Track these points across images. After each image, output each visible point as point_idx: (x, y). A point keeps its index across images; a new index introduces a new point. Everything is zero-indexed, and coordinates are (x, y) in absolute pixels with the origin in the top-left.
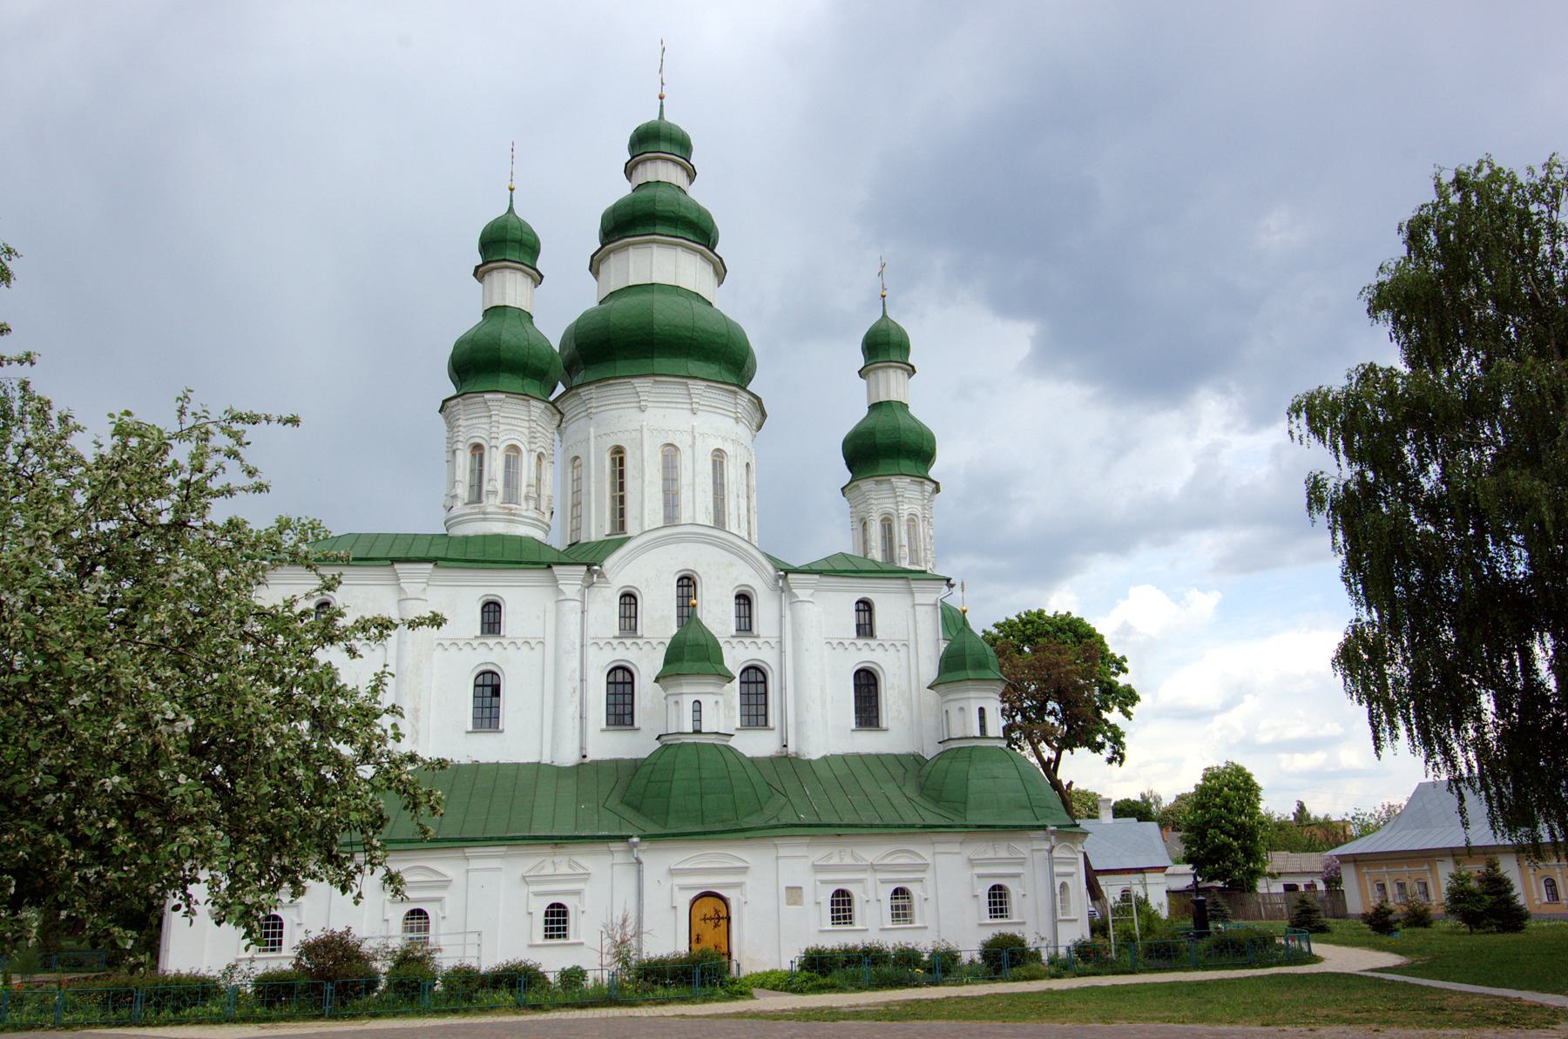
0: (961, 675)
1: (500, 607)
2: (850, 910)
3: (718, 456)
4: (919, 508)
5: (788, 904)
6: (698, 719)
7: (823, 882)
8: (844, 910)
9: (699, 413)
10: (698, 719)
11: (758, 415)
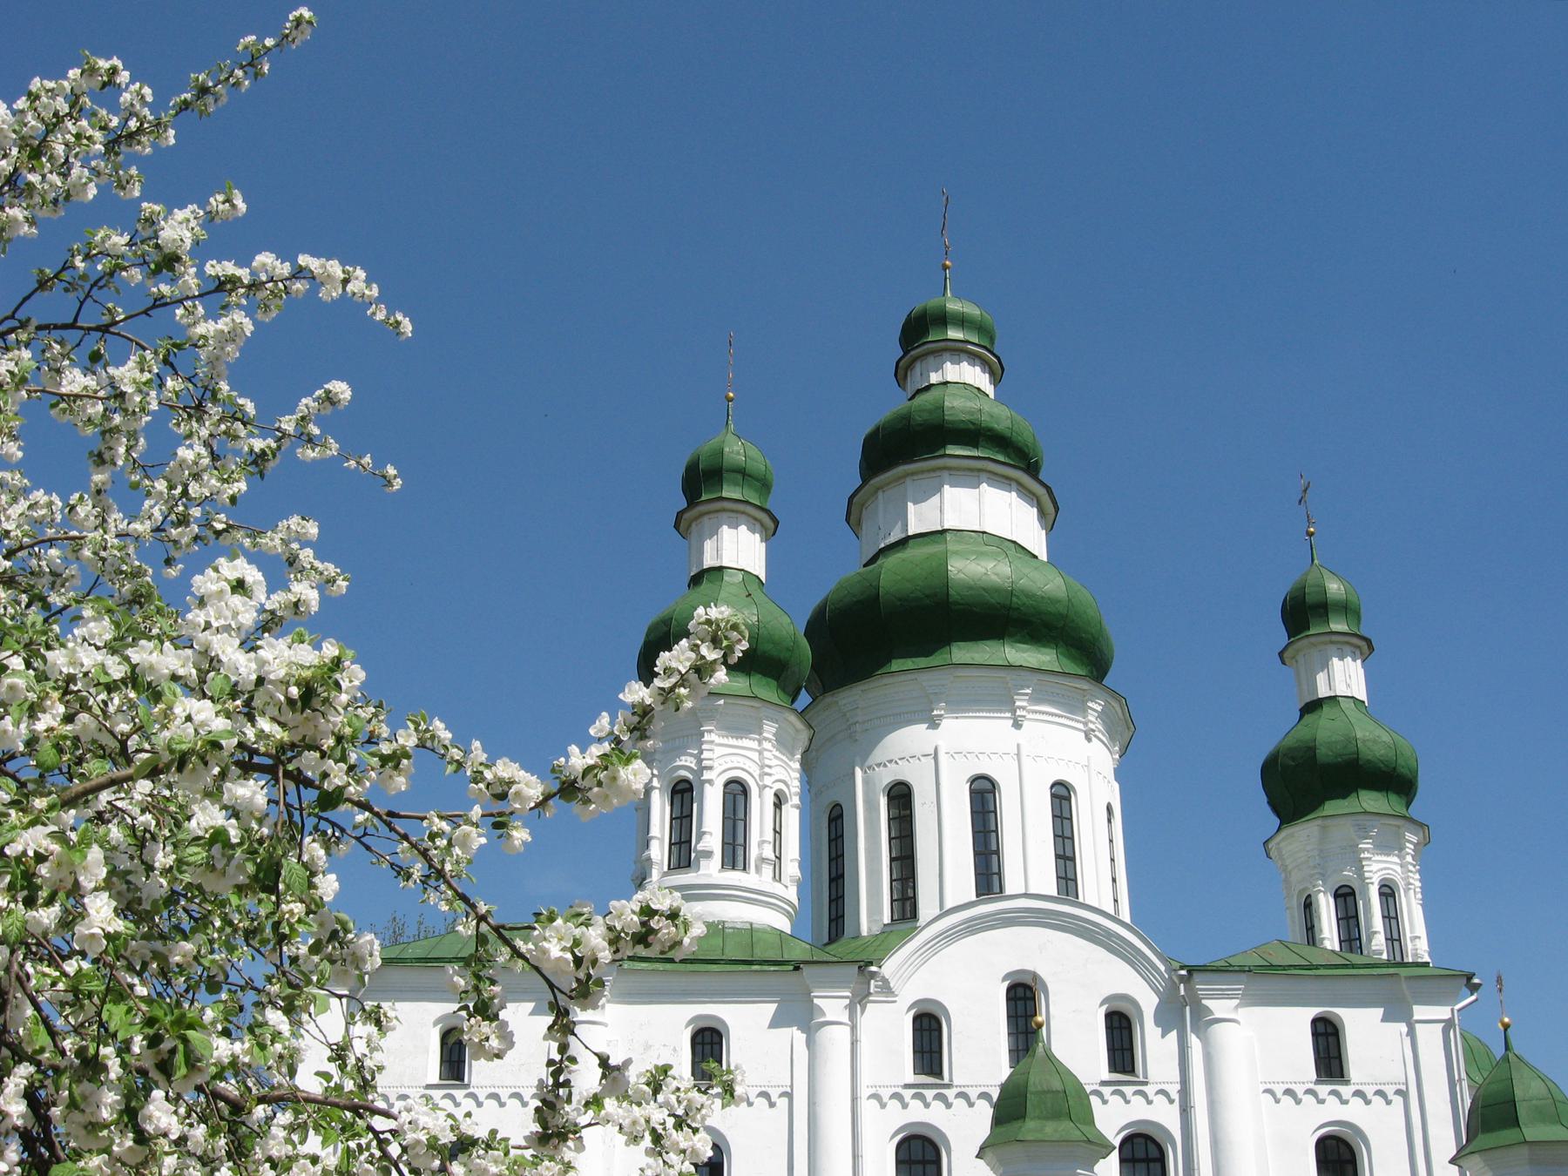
0: (1508, 1135)
1: (721, 1036)
3: (1062, 795)
4: (1398, 869)
9: (1026, 724)
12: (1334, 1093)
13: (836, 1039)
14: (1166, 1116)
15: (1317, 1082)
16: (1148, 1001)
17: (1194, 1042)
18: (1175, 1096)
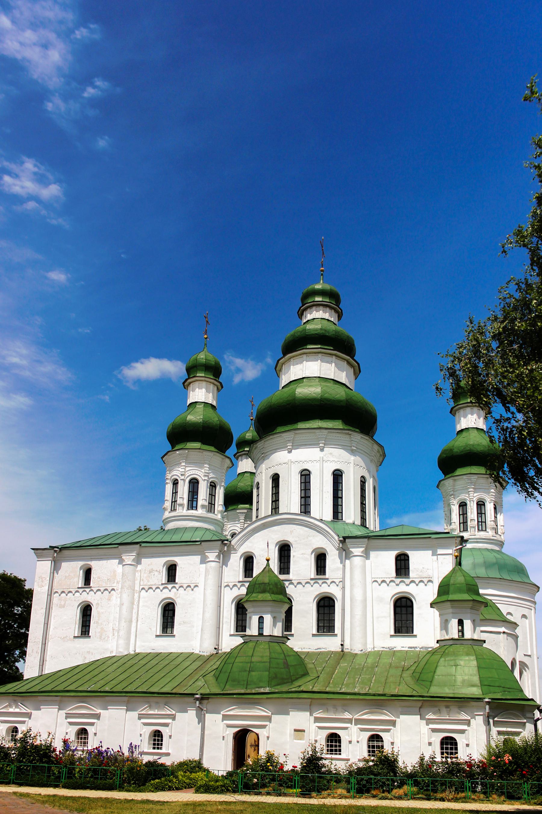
2: (340, 746)
6: (261, 628)
7: (320, 728)
8: (336, 746)
10: (261, 628)
11: (376, 447)
15: (396, 578)
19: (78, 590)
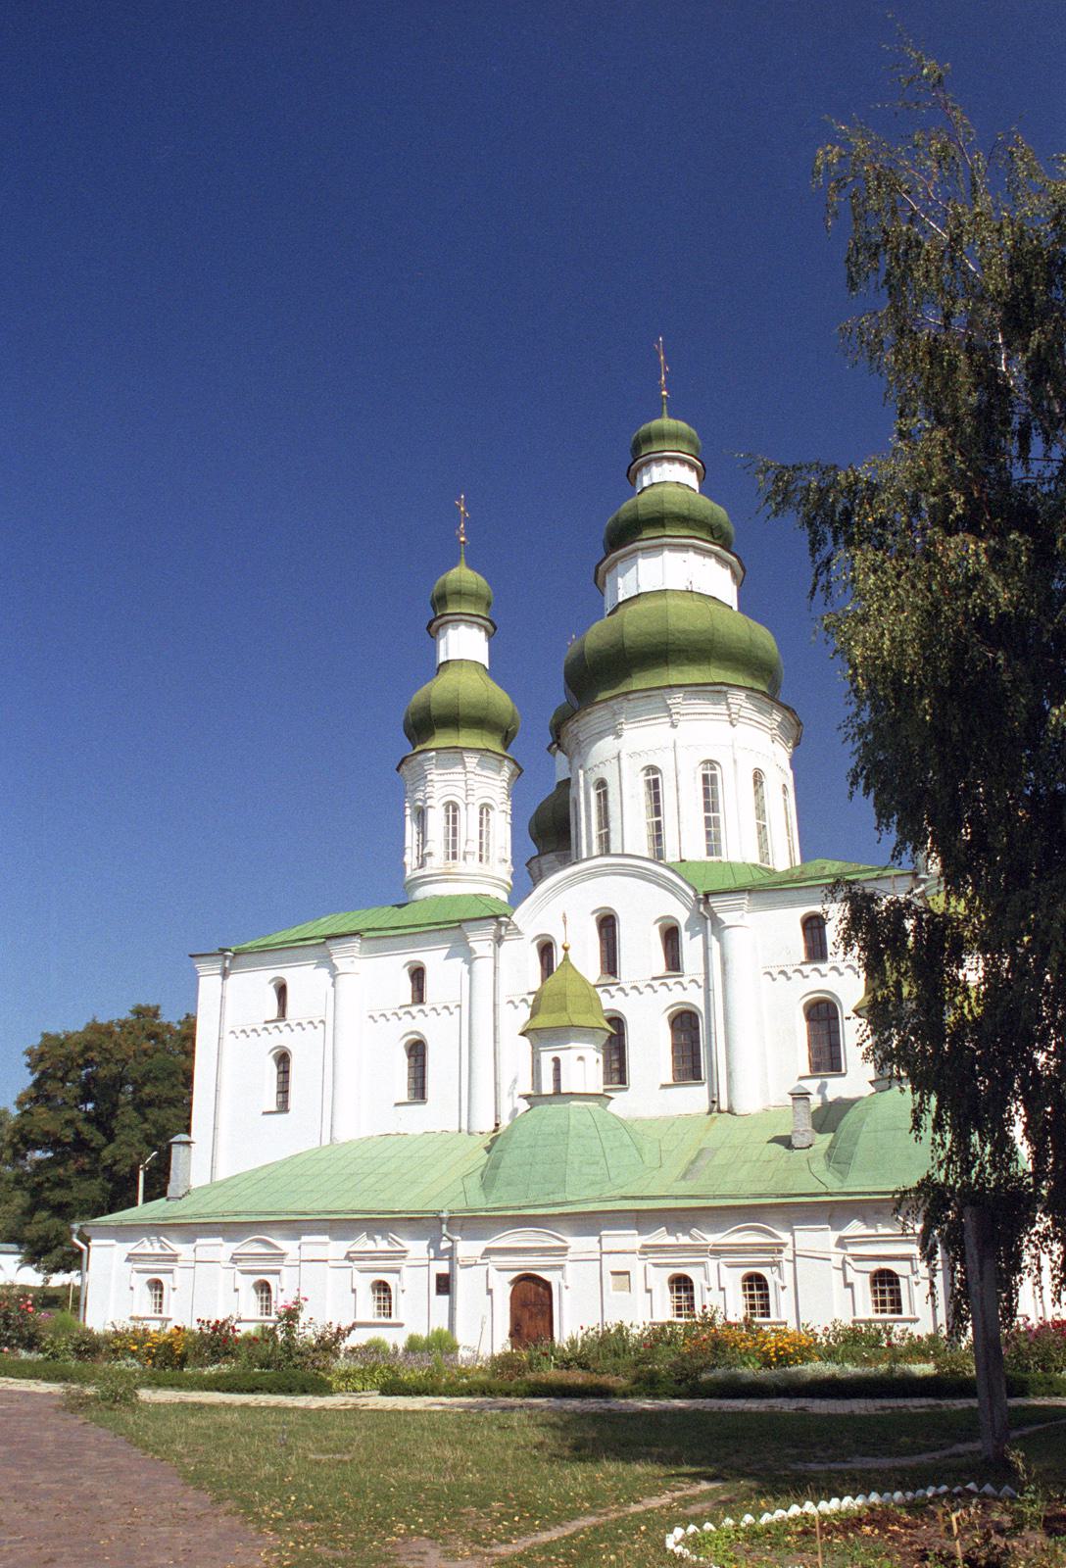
5: (614, 1290)
6: (557, 1080)
9: (680, 724)
10: (557, 1080)
12: (816, 969)
13: (483, 967)
14: (695, 998)
16: (682, 915)
17: (713, 941)
18: (701, 983)
19: (267, 1026)
